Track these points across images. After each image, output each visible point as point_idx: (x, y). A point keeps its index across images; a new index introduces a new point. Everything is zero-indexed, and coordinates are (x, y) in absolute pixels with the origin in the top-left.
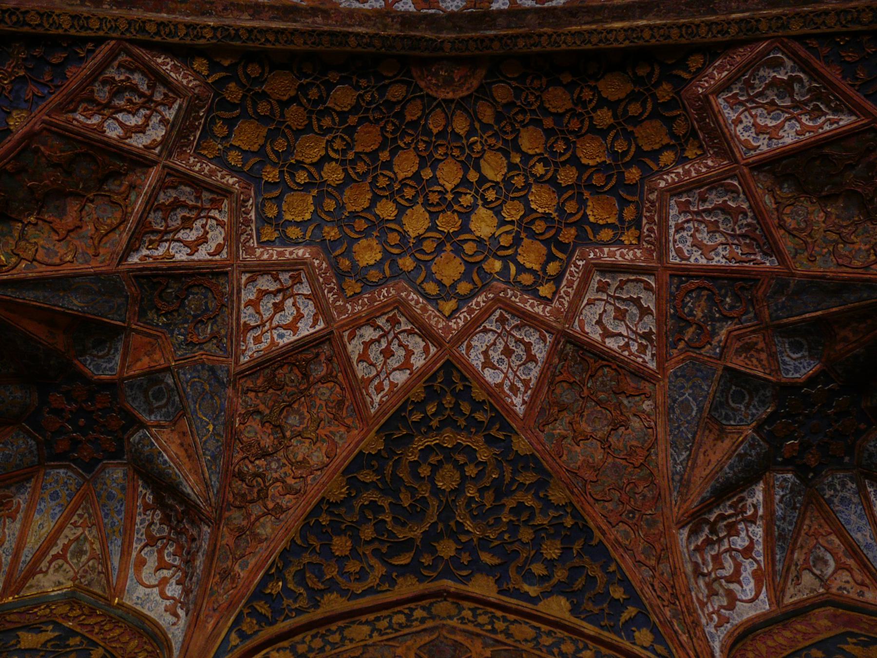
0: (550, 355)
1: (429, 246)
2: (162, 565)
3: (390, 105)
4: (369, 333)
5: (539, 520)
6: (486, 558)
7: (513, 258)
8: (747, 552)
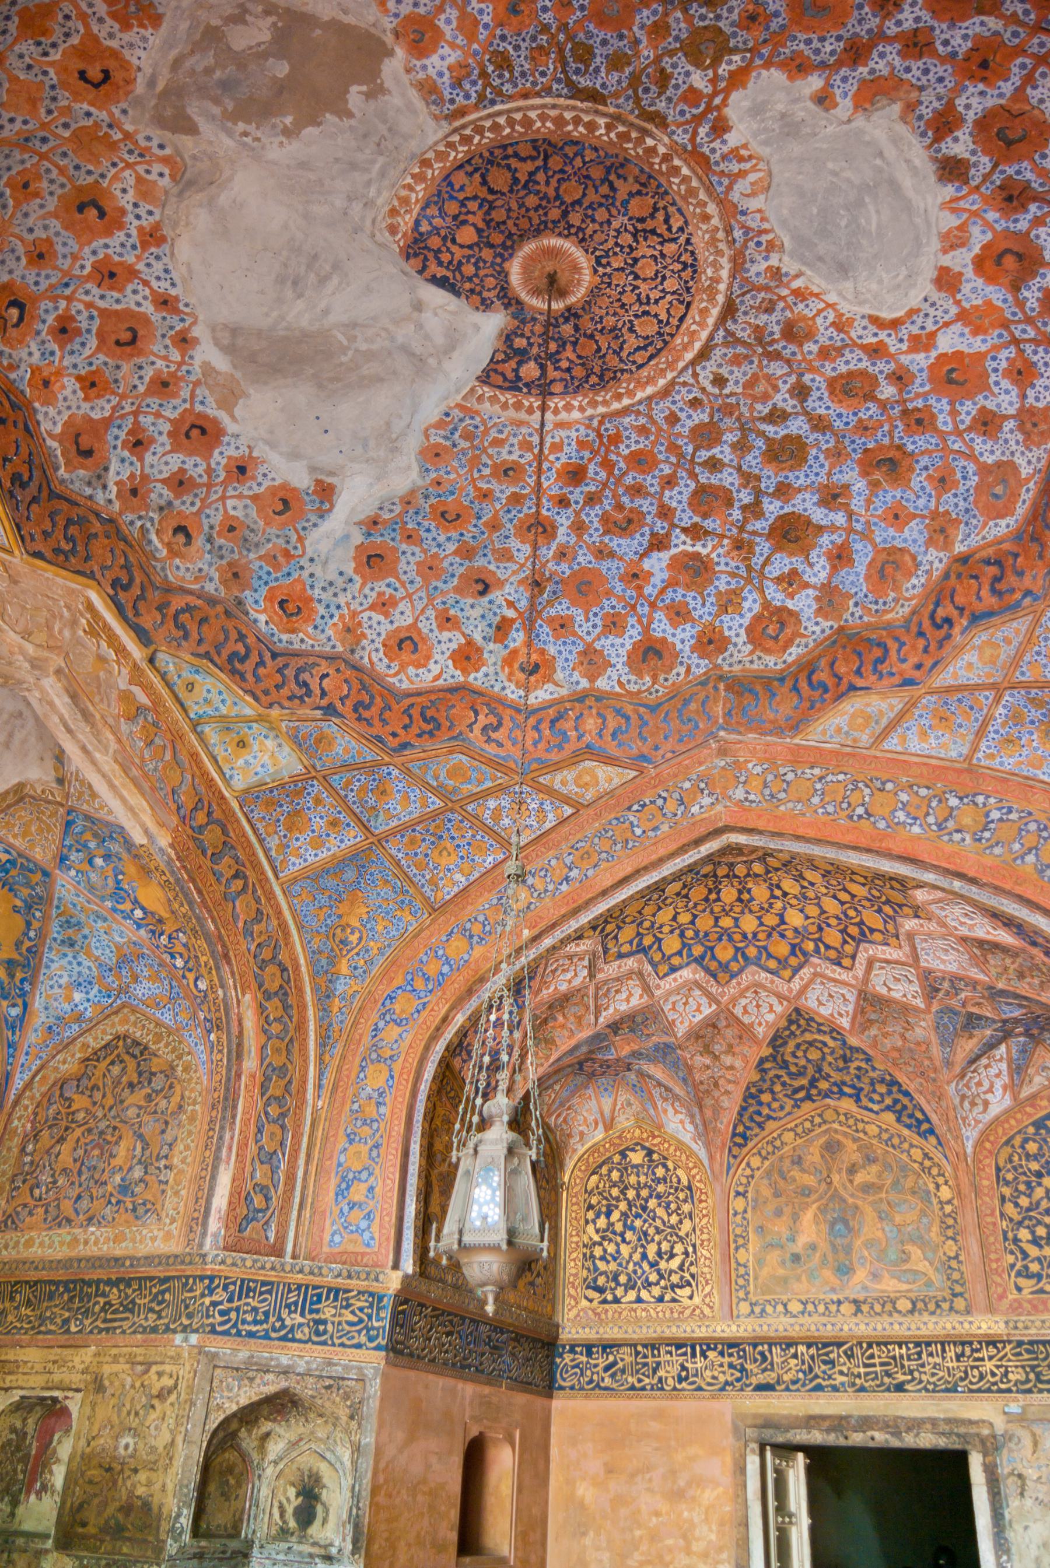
0: (857, 1003)
1: (761, 936)
2: (676, 1112)
3: (705, 876)
4: (743, 1002)
5: (871, 1074)
6: (846, 1090)
7: (820, 940)
8: (998, 1076)
